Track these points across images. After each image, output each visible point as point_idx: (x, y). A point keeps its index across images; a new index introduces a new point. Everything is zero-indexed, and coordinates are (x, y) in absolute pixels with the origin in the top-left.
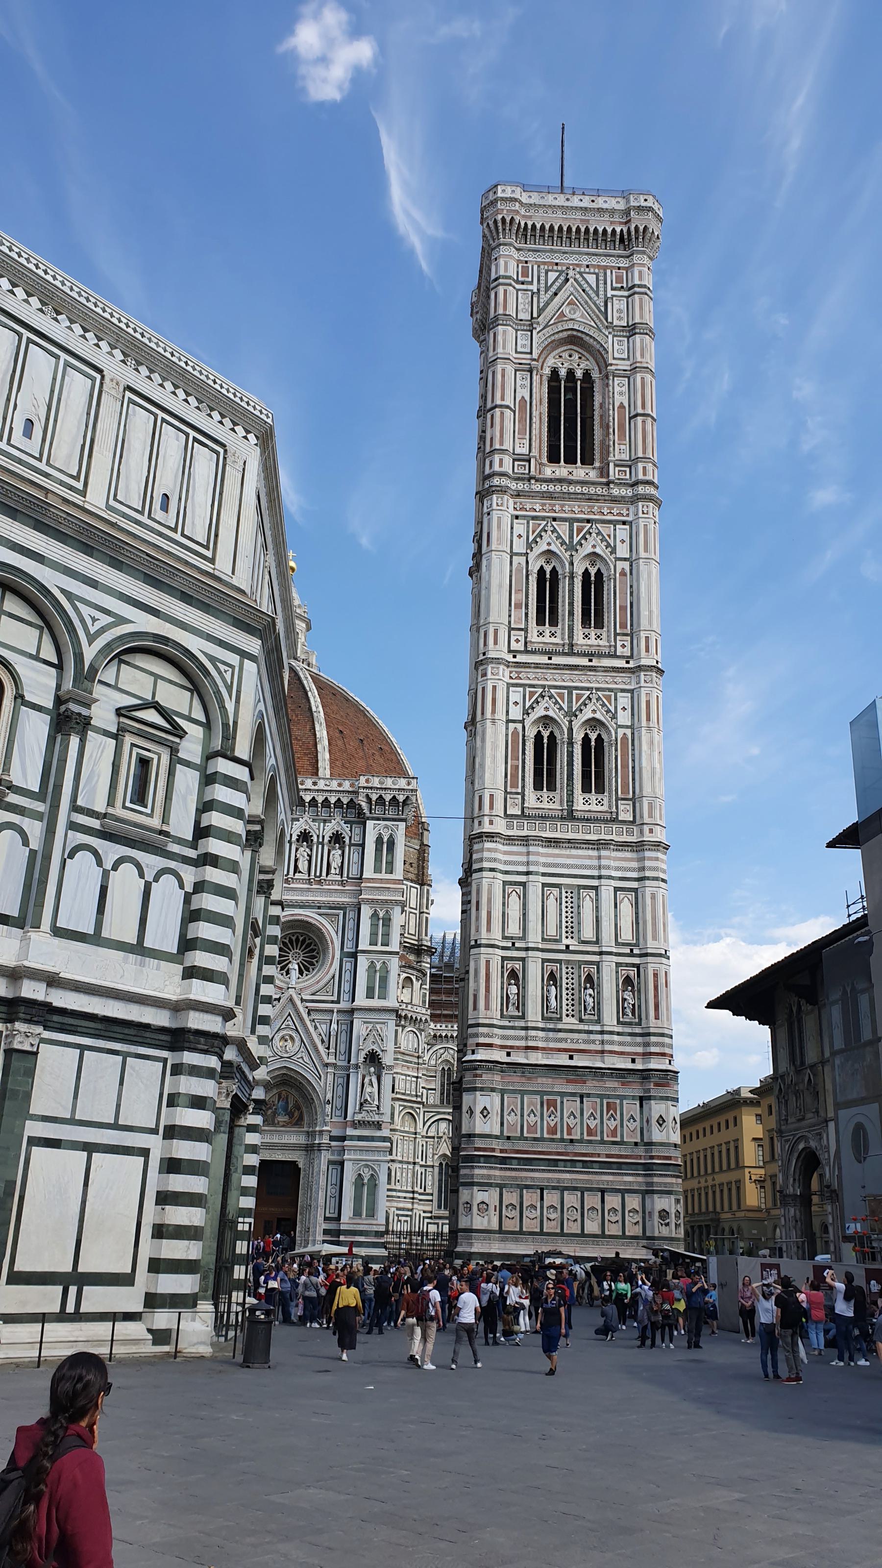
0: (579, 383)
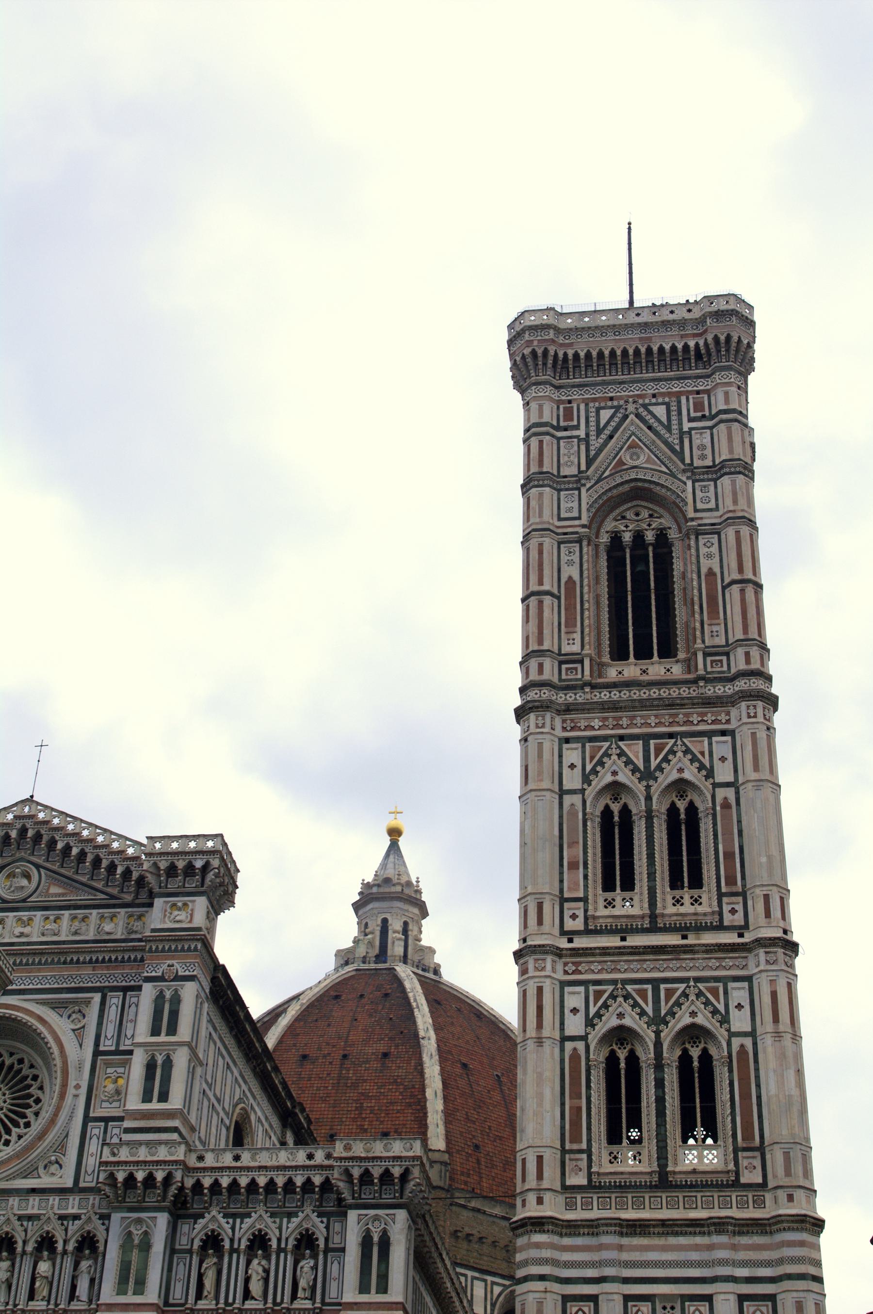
0: (650, 549)
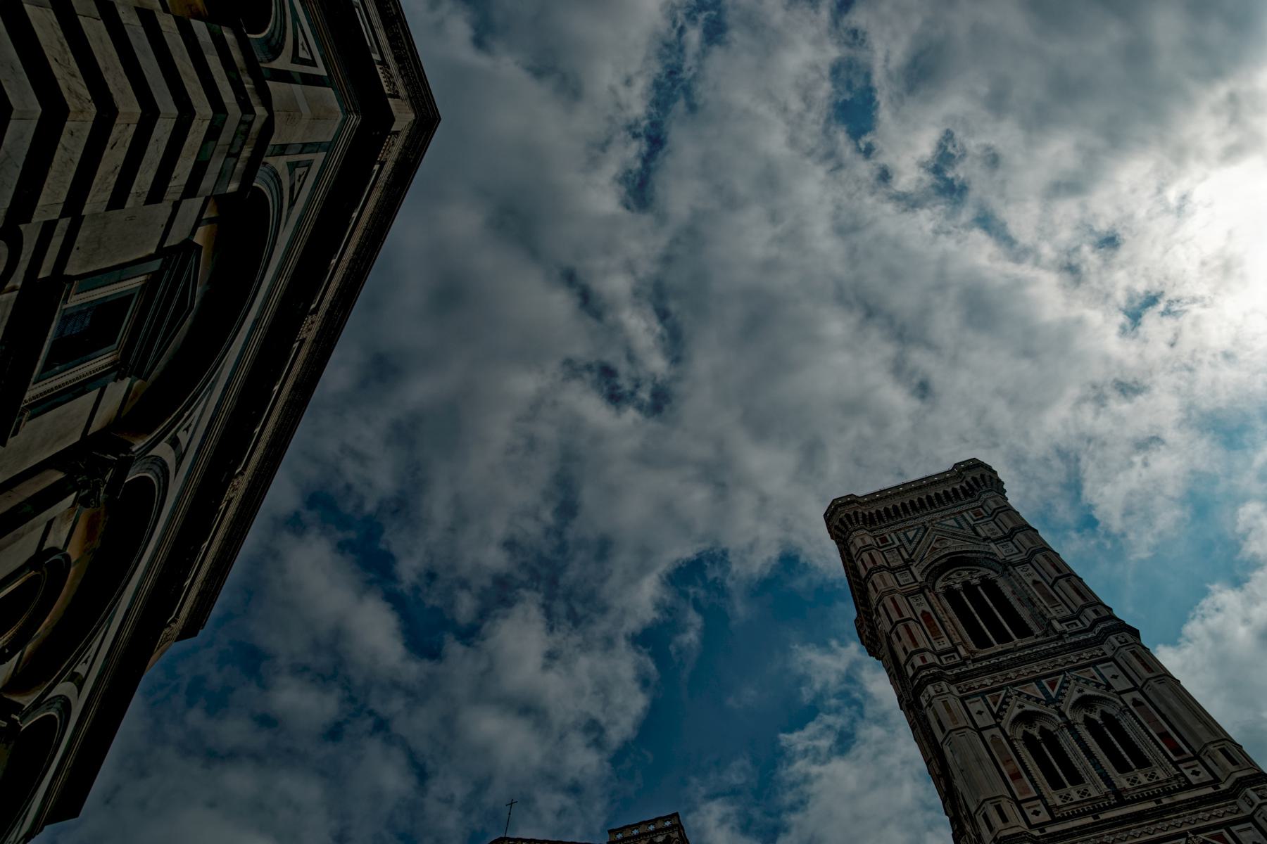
0: (979, 588)
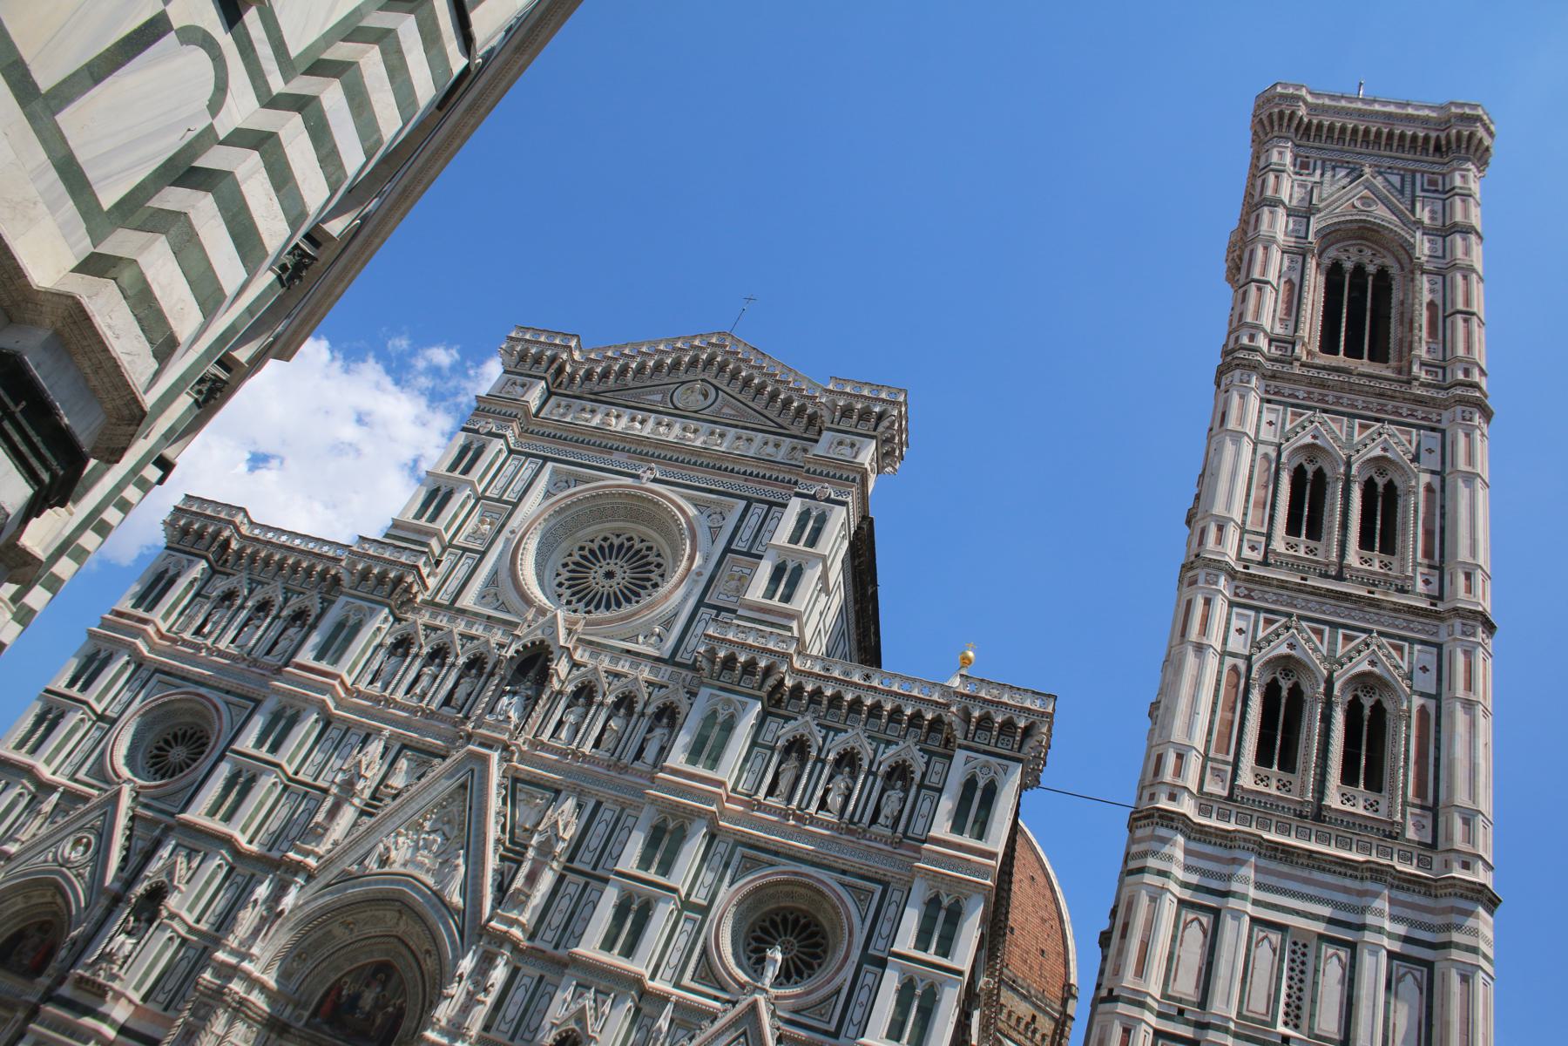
0: (1370, 278)
